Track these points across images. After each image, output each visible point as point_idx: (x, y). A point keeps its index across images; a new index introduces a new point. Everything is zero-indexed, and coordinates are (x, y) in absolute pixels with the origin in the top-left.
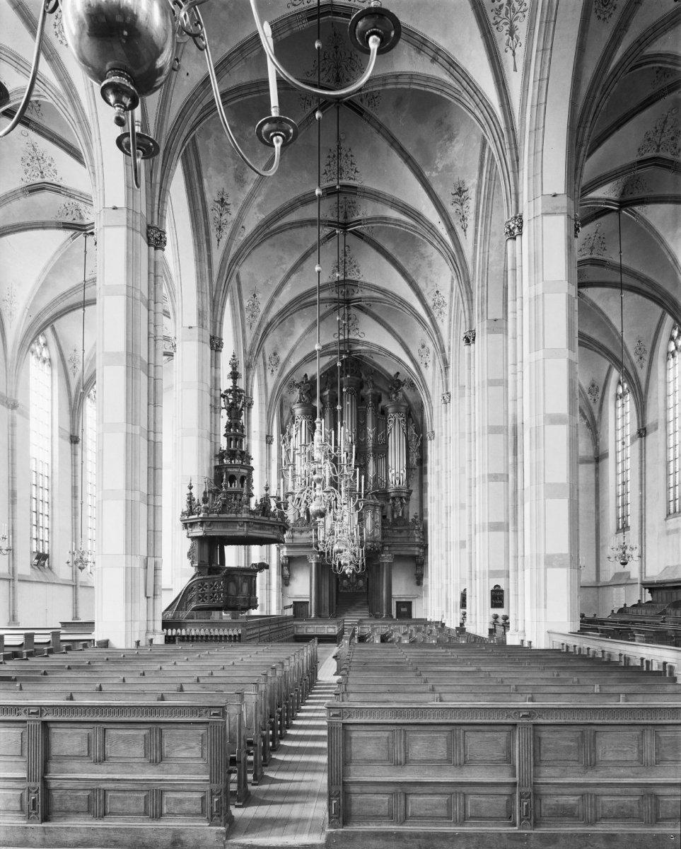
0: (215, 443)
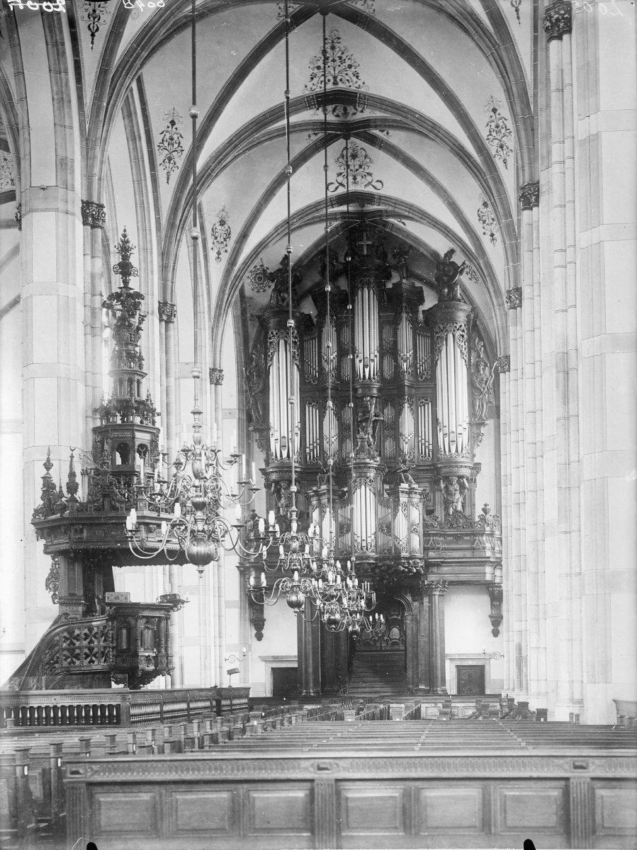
0: (94, 388)
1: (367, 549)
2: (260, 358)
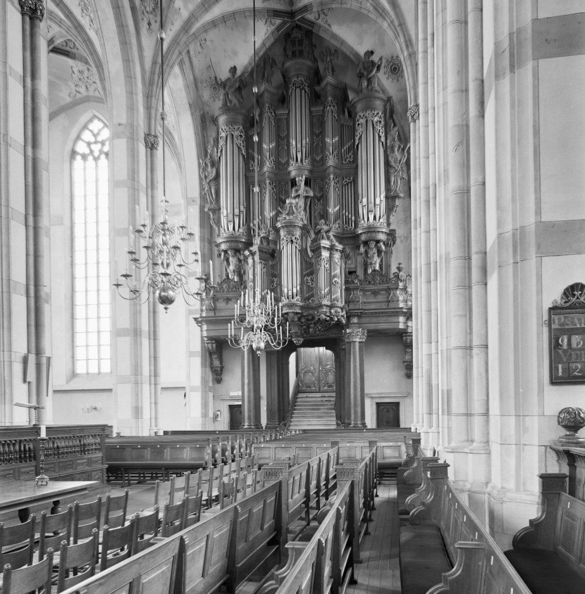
1: (293, 298)
2: (213, 151)
